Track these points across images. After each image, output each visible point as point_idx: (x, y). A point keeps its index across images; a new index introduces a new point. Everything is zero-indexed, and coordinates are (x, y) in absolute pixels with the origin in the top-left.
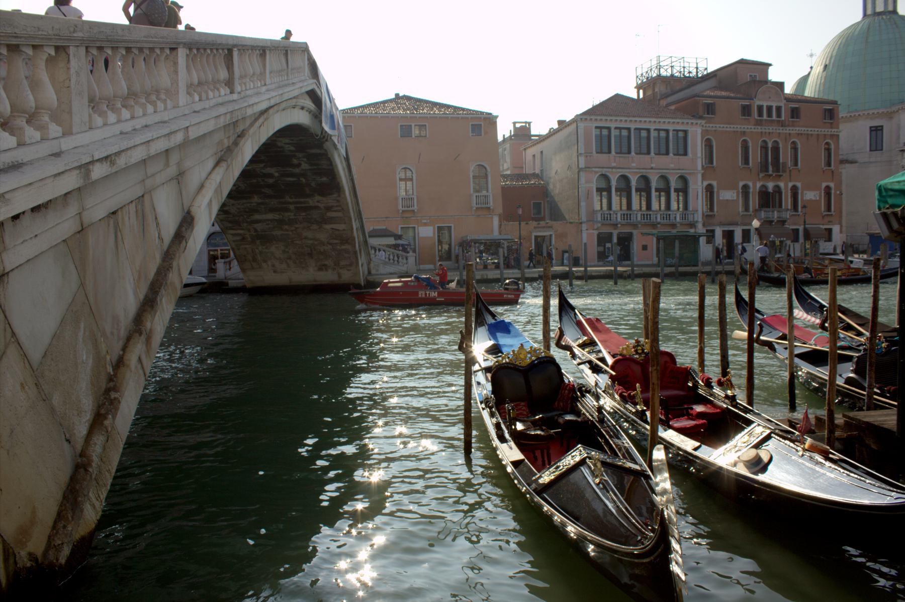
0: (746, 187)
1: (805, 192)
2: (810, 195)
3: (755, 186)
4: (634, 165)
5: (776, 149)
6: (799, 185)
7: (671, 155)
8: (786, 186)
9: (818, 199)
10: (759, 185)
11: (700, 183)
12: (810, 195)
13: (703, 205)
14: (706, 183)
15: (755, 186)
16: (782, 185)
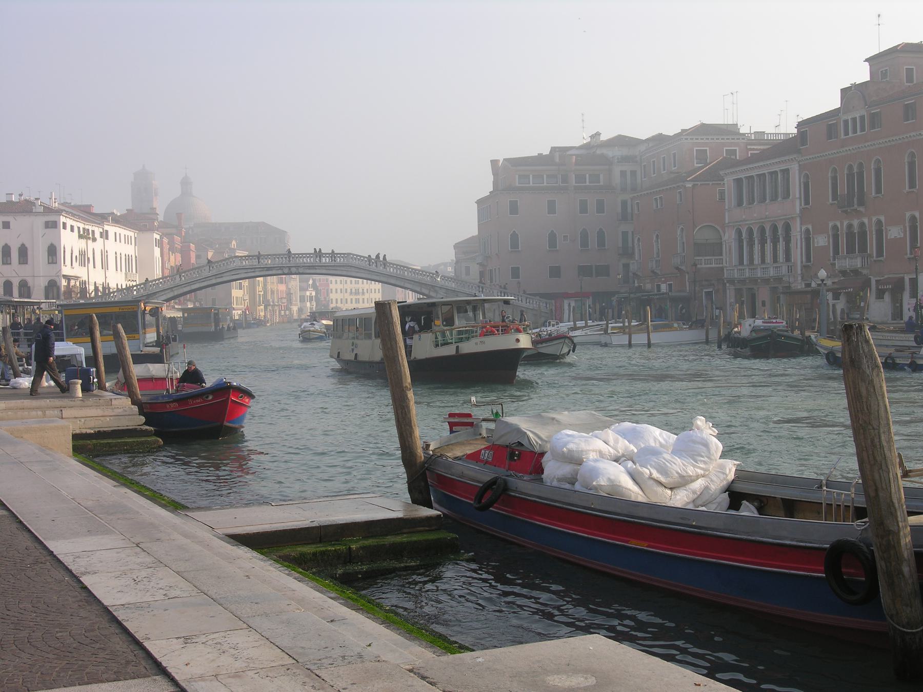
0: (835, 228)
1: (889, 228)
2: (894, 232)
4: (755, 215)
5: (860, 174)
6: (882, 218)
8: (870, 221)
10: (845, 224)
11: (799, 229)
12: (894, 232)
16: (866, 221)
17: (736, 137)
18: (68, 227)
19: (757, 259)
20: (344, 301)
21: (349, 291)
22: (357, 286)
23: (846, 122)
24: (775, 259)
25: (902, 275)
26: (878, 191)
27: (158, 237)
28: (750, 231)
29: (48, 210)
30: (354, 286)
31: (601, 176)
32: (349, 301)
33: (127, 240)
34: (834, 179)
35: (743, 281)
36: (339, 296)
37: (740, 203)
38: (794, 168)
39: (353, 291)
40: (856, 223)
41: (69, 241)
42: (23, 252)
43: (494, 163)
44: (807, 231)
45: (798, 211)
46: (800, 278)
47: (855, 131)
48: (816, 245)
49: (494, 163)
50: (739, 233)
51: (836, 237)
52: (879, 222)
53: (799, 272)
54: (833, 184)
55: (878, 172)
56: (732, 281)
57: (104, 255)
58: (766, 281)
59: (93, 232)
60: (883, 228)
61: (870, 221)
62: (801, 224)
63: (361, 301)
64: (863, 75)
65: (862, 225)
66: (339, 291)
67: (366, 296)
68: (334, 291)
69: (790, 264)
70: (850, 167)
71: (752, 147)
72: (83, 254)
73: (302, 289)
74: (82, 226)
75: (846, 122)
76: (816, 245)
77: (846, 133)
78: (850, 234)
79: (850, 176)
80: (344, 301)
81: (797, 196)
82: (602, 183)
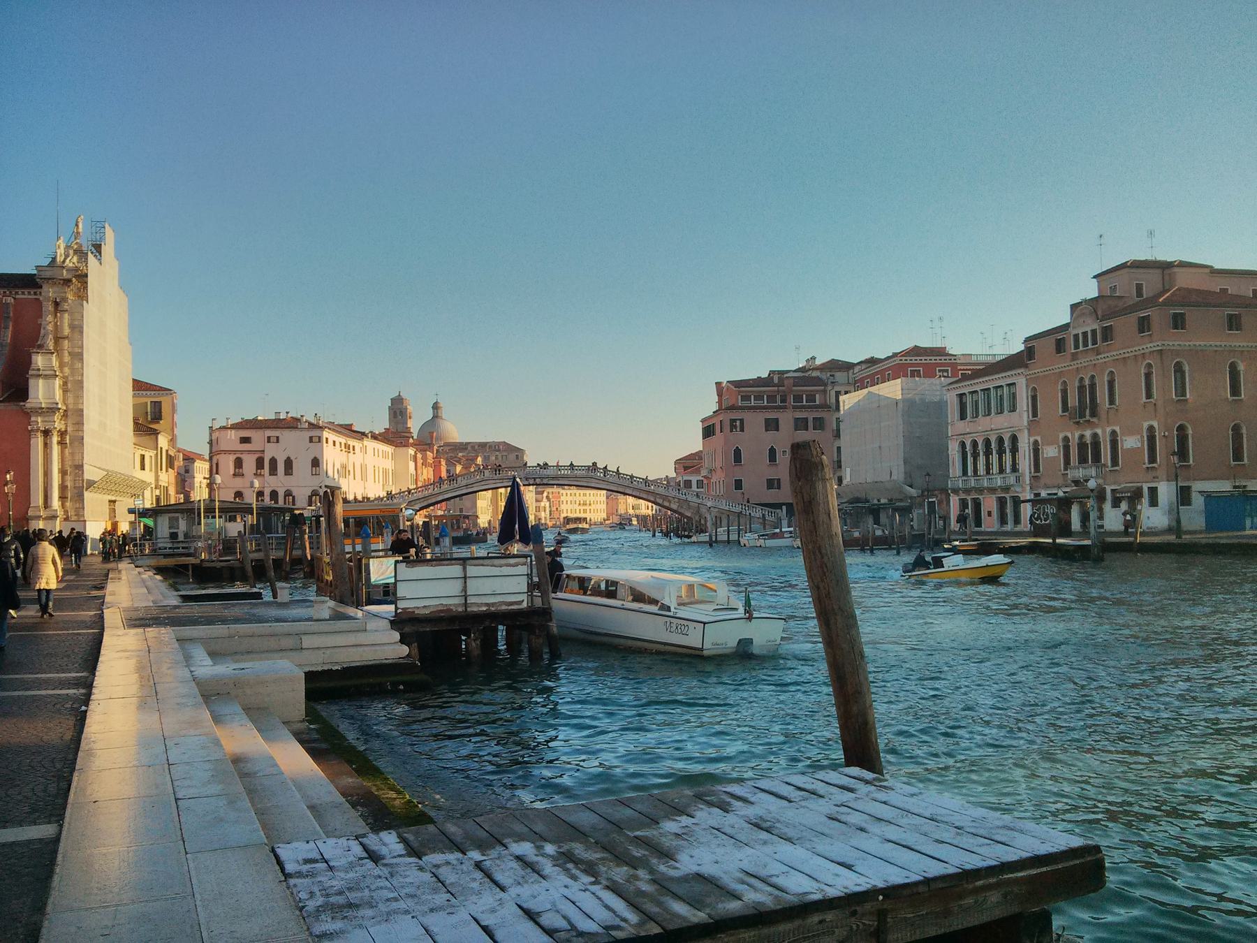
0: (1066, 439)
1: (1124, 438)
2: (1130, 442)
3: (1073, 435)
5: (1093, 386)
6: (1117, 429)
7: (1006, 412)
8: (1104, 432)
9: (1140, 446)
11: (1027, 441)
13: (1030, 465)
14: (1032, 439)
15: (1074, 436)
16: (1099, 431)
17: (948, 358)
18: (330, 442)
19: (995, 469)
20: (573, 511)
21: (578, 502)
22: (585, 498)
23: (1076, 336)
24: (1002, 471)
25: (1139, 484)
26: (1112, 401)
27: (413, 453)
28: (975, 443)
29: (312, 426)
30: (582, 499)
31: (817, 396)
32: (578, 511)
33: (385, 455)
34: (1064, 392)
35: (967, 491)
36: (569, 507)
37: (963, 416)
38: (1021, 382)
39: (582, 502)
40: (1088, 434)
41: (333, 454)
42: (289, 464)
43: (718, 384)
44: (1036, 442)
45: (1026, 423)
46: (1028, 488)
47: (1085, 345)
48: (1045, 456)
49: (718, 384)
50: (963, 445)
51: (1067, 448)
52: (1114, 433)
53: (1028, 482)
54: (1062, 397)
55: (1111, 384)
56: (956, 491)
57: (364, 468)
58: (992, 490)
59: (354, 447)
60: (1119, 438)
61: (1104, 432)
62: (1029, 436)
63: (588, 511)
64: (1092, 291)
65: (1095, 436)
66: (569, 502)
67: (593, 507)
68: (565, 502)
69: (1017, 474)
70: (1082, 379)
71: (962, 368)
72: (344, 467)
73: (537, 501)
74: (343, 441)
75: (1076, 336)
76: (1045, 456)
77: (1077, 347)
78: (1082, 446)
79: (1081, 388)
80: (573, 511)
81: (1025, 409)
82: (817, 403)
